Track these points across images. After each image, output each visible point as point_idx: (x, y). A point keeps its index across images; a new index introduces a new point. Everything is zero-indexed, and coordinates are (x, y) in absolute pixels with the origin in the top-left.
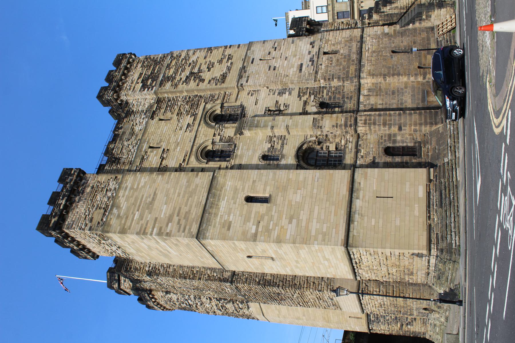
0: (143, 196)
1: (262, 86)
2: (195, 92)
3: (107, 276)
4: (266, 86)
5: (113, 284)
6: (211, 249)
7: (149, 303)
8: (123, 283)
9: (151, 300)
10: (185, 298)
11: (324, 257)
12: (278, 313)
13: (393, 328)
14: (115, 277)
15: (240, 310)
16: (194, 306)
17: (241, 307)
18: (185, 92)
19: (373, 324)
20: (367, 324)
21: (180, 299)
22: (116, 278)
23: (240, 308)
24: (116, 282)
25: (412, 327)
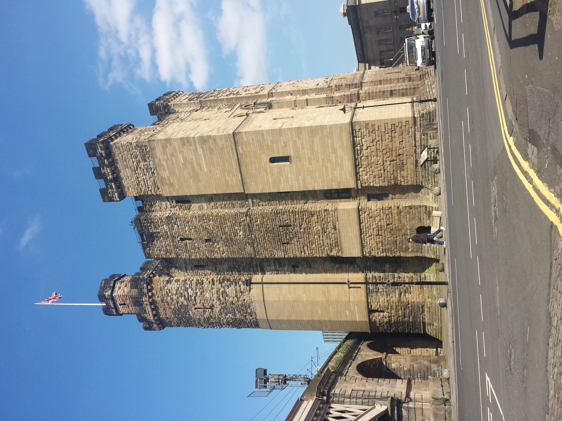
0: (187, 127)
1: (288, 93)
2: (234, 100)
3: (101, 284)
4: (291, 92)
5: (106, 292)
6: (241, 152)
7: (144, 300)
8: (117, 290)
9: (148, 293)
10: (185, 287)
11: (333, 145)
12: (278, 292)
13: (392, 298)
14: (110, 284)
15: (241, 294)
16: (193, 298)
17: (242, 290)
18: (225, 100)
19: (372, 296)
20: (366, 294)
21: (180, 289)
22: (111, 285)
23: (241, 292)
24: (110, 289)
25: (410, 295)
